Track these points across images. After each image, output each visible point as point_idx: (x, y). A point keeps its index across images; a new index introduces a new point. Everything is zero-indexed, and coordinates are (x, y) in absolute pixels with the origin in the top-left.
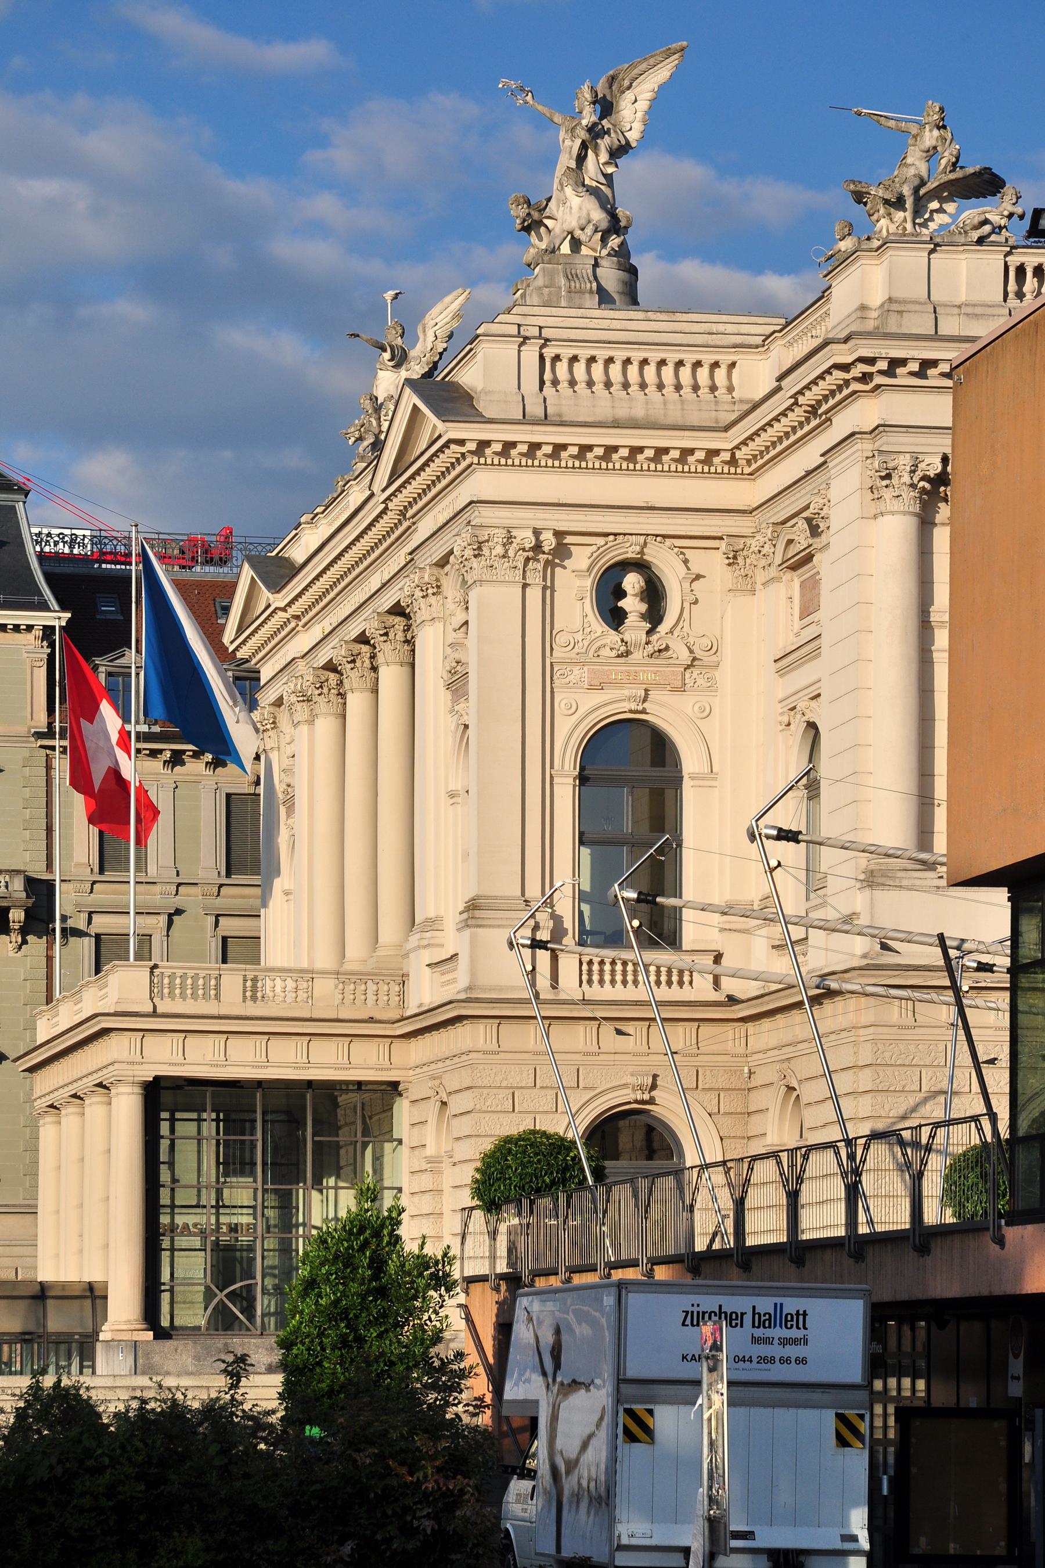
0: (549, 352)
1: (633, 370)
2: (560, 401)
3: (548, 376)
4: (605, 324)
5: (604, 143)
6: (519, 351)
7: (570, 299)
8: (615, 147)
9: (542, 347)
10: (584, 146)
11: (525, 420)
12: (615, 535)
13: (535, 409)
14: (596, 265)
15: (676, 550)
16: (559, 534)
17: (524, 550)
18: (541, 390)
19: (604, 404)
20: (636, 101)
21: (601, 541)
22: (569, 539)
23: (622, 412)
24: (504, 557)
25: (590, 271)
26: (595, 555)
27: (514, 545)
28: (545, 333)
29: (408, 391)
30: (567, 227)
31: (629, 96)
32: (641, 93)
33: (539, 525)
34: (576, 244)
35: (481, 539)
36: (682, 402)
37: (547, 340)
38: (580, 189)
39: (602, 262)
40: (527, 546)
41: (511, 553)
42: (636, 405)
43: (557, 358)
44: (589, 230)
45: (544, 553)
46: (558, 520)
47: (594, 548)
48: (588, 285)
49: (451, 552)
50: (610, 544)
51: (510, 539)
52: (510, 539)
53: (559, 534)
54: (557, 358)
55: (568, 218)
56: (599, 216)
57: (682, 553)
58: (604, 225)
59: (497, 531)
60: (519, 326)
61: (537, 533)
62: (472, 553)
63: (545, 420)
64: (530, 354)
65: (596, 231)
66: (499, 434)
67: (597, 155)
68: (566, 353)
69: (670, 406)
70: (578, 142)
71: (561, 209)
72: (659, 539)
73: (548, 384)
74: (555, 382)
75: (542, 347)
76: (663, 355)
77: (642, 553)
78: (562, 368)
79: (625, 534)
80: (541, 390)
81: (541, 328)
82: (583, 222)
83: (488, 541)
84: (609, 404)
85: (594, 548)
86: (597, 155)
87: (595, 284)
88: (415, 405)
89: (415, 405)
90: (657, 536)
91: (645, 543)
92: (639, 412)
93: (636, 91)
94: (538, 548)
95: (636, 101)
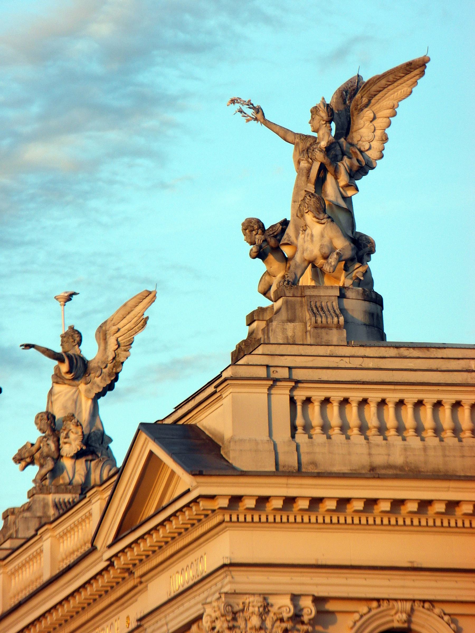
0: (300, 395)
1: (390, 411)
2: (317, 449)
3: (299, 421)
4: (356, 362)
5: (344, 165)
6: (269, 395)
7: (318, 336)
8: (355, 168)
9: (293, 389)
10: (323, 169)
11: (279, 472)
12: (378, 600)
13: (288, 459)
14: (342, 296)
15: (446, 618)
16: (318, 600)
17: (282, 620)
18: (293, 437)
19: (358, 451)
20: (374, 118)
21: (363, 609)
22: (330, 606)
23: (380, 459)
24: (261, 628)
25: (335, 304)
26: (358, 624)
27: (271, 615)
28: (298, 374)
29: (143, 436)
30: (307, 256)
31: (368, 113)
32: (380, 110)
33: (297, 590)
34: (318, 273)
35: (236, 608)
36: (444, 449)
37: (297, 382)
38: (321, 216)
39: (349, 294)
40: (286, 616)
41: (268, 624)
42: (395, 451)
43: (308, 400)
44: (333, 259)
45: (303, 623)
46: (317, 585)
47: (357, 616)
48: (336, 319)
49: (199, 618)
50: (373, 612)
51: (266, 607)
52: (266, 607)
53: (318, 600)
54: (308, 400)
55: (308, 245)
56: (341, 243)
57: (454, 621)
58: (348, 254)
59: (251, 599)
60: (268, 366)
61: (295, 598)
62: (225, 625)
63: (299, 472)
64: (281, 397)
65: (339, 261)
66: (251, 489)
67: (336, 178)
68: (318, 395)
69: (431, 453)
70: (316, 167)
71: (301, 236)
72: (427, 605)
73: (300, 430)
74: (307, 428)
75: (293, 389)
76: (420, 396)
77: (409, 621)
78: (315, 412)
79: (388, 600)
80: (293, 437)
81: (290, 368)
82: (326, 250)
83: (243, 610)
84: (365, 450)
85: (357, 616)
86: (336, 178)
87: (342, 319)
88: (151, 453)
89: (151, 453)
90: (424, 601)
91: (412, 610)
92: (398, 458)
93: (374, 108)
94: (297, 617)
95: (374, 118)
